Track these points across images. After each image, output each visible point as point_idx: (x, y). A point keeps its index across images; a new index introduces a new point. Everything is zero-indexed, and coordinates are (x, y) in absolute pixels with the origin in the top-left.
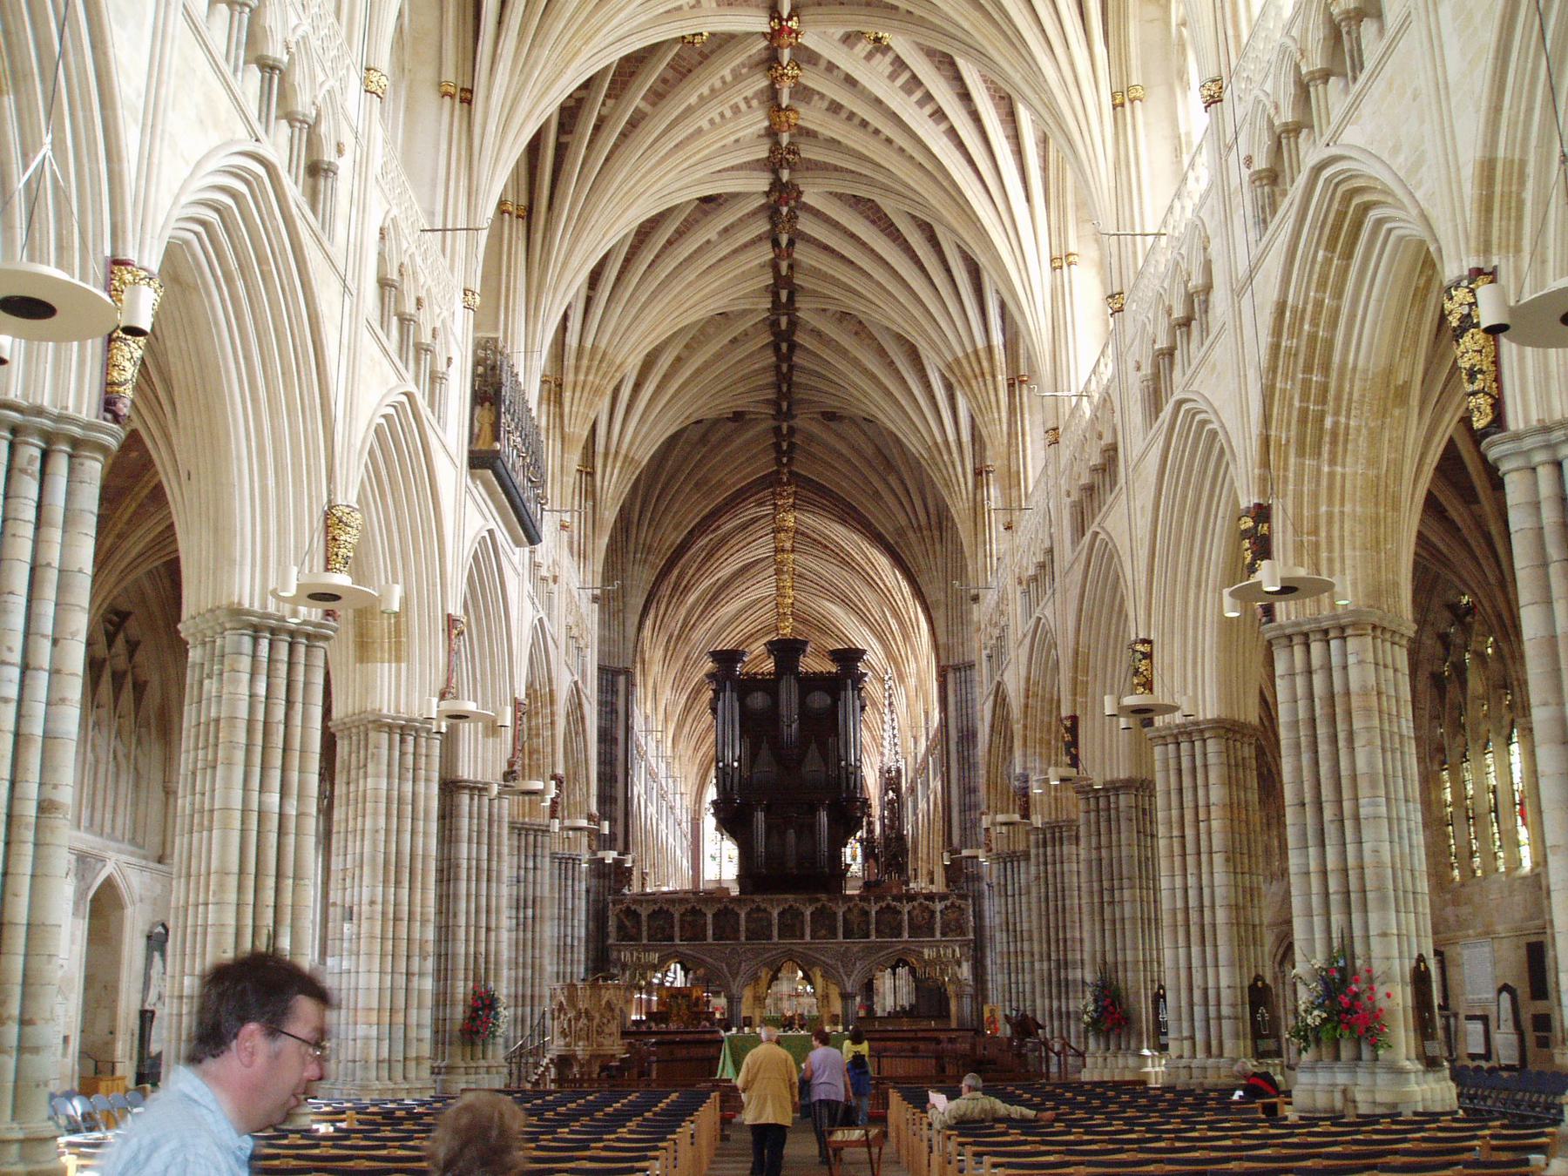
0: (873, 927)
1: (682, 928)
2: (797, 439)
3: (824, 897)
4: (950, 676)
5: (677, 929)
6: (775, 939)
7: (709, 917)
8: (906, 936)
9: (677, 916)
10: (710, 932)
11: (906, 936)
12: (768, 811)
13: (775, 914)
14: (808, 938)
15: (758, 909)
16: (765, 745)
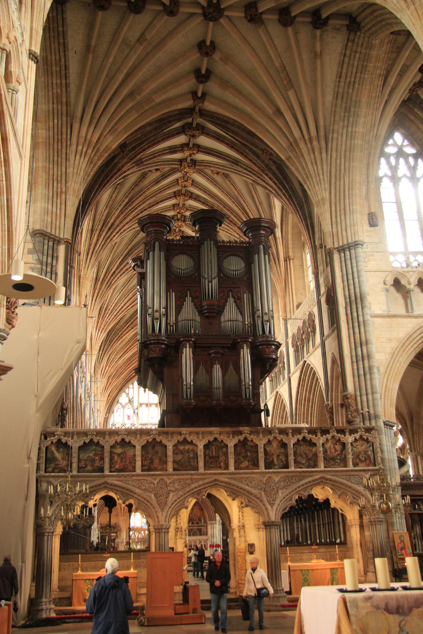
0: (291, 458)
1: (111, 460)
2: (217, 56)
3: (246, 429)
4: (336, 257)
5: (107, 460)
6: (201, 470)
7: (138, 452)
8: (322, 467)
9: (107, 448)
10: (139, 464)
11: (322, 467)
12: (195, 347)
13: (201, 447)
14: (232, 468)
15: (185, 441)
16: (189, 299)
